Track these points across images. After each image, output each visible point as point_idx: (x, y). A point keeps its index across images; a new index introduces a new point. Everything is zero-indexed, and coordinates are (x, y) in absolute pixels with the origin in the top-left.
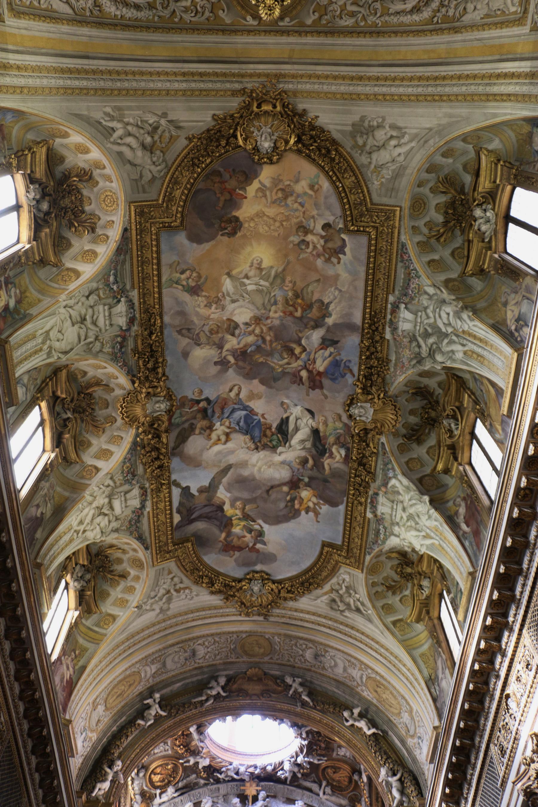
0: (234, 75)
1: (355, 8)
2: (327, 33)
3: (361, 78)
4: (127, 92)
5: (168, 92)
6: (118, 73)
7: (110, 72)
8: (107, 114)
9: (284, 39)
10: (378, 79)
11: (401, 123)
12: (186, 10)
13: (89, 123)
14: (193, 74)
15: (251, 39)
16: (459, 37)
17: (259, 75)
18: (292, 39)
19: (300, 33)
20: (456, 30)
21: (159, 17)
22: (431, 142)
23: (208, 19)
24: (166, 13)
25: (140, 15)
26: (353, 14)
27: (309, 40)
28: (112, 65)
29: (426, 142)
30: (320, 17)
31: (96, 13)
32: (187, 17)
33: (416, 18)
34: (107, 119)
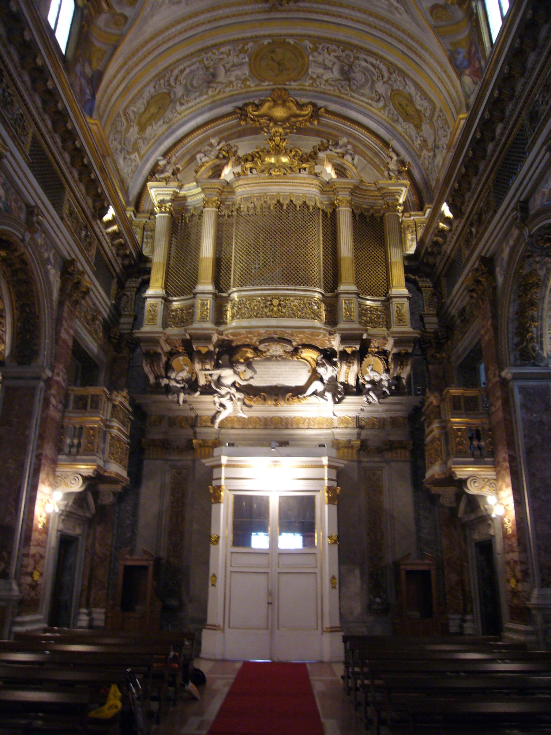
0: (303, 11)
1: (221, 57)
2: (238, 40)
3: (209, 22)
4: (382, 19)
5: (353, 9)
6: (386, 33)
7: (391, 36)
8: (398, 12)
9: (266, 33)
10: (197, 26)
11: (174, 8)
12: (334, 51)
13: (413, 16)
14: (334, 15)
15: (291, 32)
16: (153, 74)
17: (284, 11)
18: (262, 33)
19: (256, 37)
20: (156, 75)
21: (352, 51)
22: (149, 9)
23: (320, 44)
24: (347, 52)
25: (366, 57)
26: (222, 53)
27: (249, 34)
28: (389, 39)
29: (153, 6)
30: (243, 47)
31: (392, 70)
32: (334, 47)
33: (181, 67)
34: (400, 11)
